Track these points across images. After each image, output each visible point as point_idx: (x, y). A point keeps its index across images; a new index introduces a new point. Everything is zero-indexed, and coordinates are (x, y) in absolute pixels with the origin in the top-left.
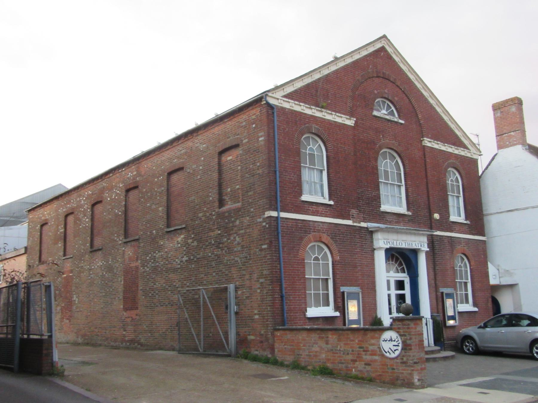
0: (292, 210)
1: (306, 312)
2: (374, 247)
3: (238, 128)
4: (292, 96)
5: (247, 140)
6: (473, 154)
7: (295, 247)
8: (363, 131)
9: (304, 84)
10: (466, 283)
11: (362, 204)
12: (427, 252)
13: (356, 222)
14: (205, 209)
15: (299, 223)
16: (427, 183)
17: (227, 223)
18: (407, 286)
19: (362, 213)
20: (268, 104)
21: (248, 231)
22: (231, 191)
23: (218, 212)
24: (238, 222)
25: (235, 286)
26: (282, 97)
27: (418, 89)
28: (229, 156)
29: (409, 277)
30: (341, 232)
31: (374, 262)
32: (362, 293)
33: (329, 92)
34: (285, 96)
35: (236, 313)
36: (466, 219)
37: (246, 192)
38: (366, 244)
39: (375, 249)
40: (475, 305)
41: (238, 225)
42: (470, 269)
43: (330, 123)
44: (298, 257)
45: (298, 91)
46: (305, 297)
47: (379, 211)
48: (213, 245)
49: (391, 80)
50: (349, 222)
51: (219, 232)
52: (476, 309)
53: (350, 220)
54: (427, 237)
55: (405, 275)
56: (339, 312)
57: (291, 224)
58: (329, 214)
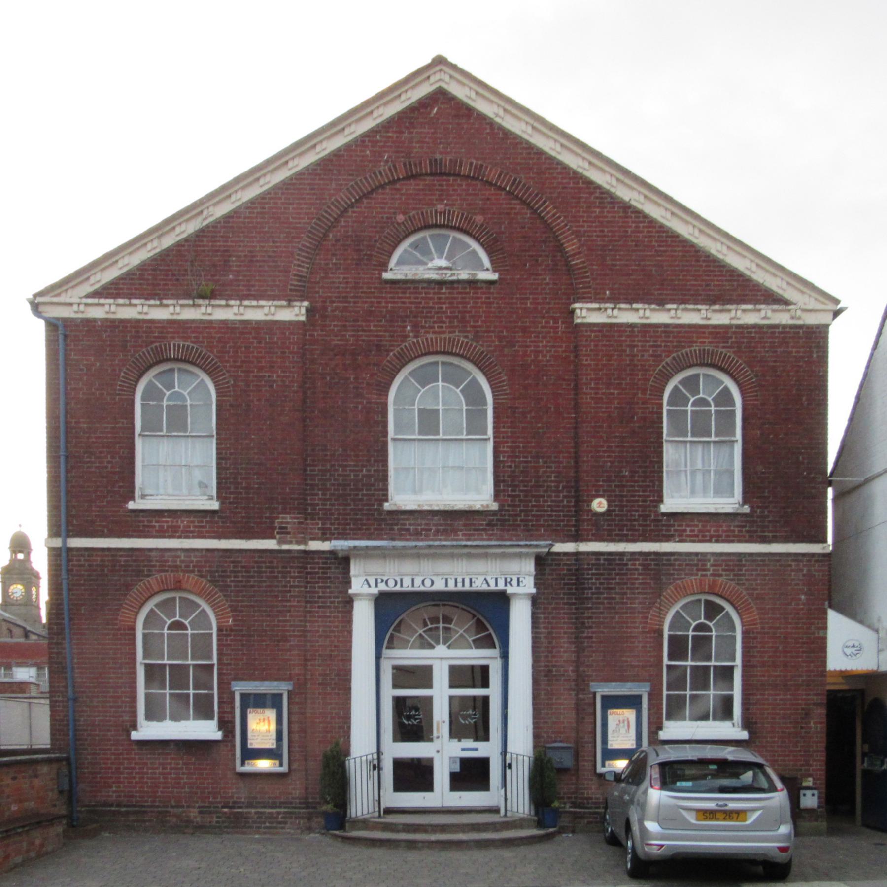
0: (103, 531)
4: (116, 289)
6: (799, 313)
11: (320, 499)
13: (291, 542)
15: (121, 556)
19: (319, 519)
33: (230, 256)
36: (746, 500)
43: (228, 328)
44: (116, 624)
45: (135, 274)
47: (380, 511)
50: (270, 544)
53: (273, 537)
57: (99, 559)
58: (207, 532)
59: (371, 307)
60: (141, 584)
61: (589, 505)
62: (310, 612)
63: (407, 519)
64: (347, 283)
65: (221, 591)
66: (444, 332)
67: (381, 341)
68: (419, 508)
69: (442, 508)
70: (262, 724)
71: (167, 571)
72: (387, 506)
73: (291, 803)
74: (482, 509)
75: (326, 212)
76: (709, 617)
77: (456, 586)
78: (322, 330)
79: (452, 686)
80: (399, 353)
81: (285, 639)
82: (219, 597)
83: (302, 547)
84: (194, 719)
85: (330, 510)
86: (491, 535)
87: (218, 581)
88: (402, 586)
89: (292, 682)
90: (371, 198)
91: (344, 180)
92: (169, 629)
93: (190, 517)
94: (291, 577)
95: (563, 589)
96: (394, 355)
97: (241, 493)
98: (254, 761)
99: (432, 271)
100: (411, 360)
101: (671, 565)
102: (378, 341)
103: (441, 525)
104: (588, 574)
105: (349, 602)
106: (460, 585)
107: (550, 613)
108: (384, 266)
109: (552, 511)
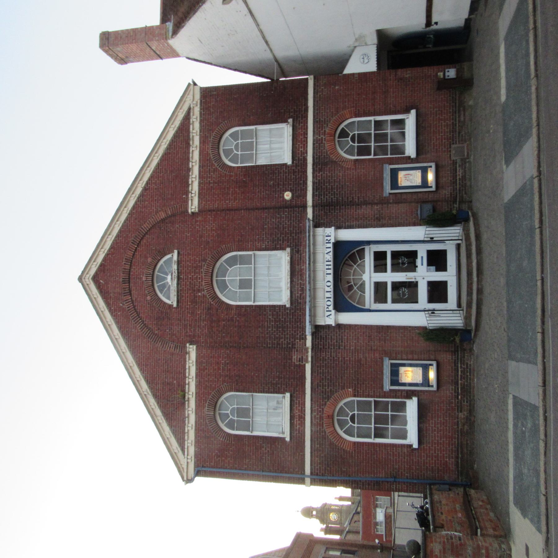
0: (302, 455)
7: (341, 455)
9: (164, 421)
11: (285, 340)
13: (307, 356)
16: (246, 209)
19: (295, 341)
38: (331, 337)
44: (352, 452)
47: (290, 309)
50: (308, 367)
53: (305, 365)
58: (302, 400)
59: (189, 313)
60: (330, 437)
62: (345, 347)
63: (295, 295)
64: (178, 324)
65: (333, 394)
66: (202, 276)
67: (206, 308)
68: (289, 289)
69: (289, 277)
70: (408, 375)
71: (323, 423)
72: (288, 305)
73: (455, 360)
74: (290, 256)
75: (145, 334)
76: (347, 135)
77: (330, 269)
78: (201, 337)
79: (386, 271)
80: (211, 299)
81: (359, 361)
82: (336, 395)
83: (310, 350)
85: (290, 335)
86: (303, 251)
87: (328, 396)
88: (330, 298)
89: (384, 358)
90: (140, 312)
91: (131, 325)
92: (354, 423)
93: (294, 409)
94: (326, 356)
95: (332, 213)
96: (213, 301)
97: (281, 381)
98: (430, 380)
99: (173, 283)
100: (215, 293)
101: (319, 157)
102: (206, 310)
103: (298, 277)
104: (324, 200)
105: (339, 326)
106: (330, 267)
107: (345, 220)
108: (170, 306)
109: (291, 220)
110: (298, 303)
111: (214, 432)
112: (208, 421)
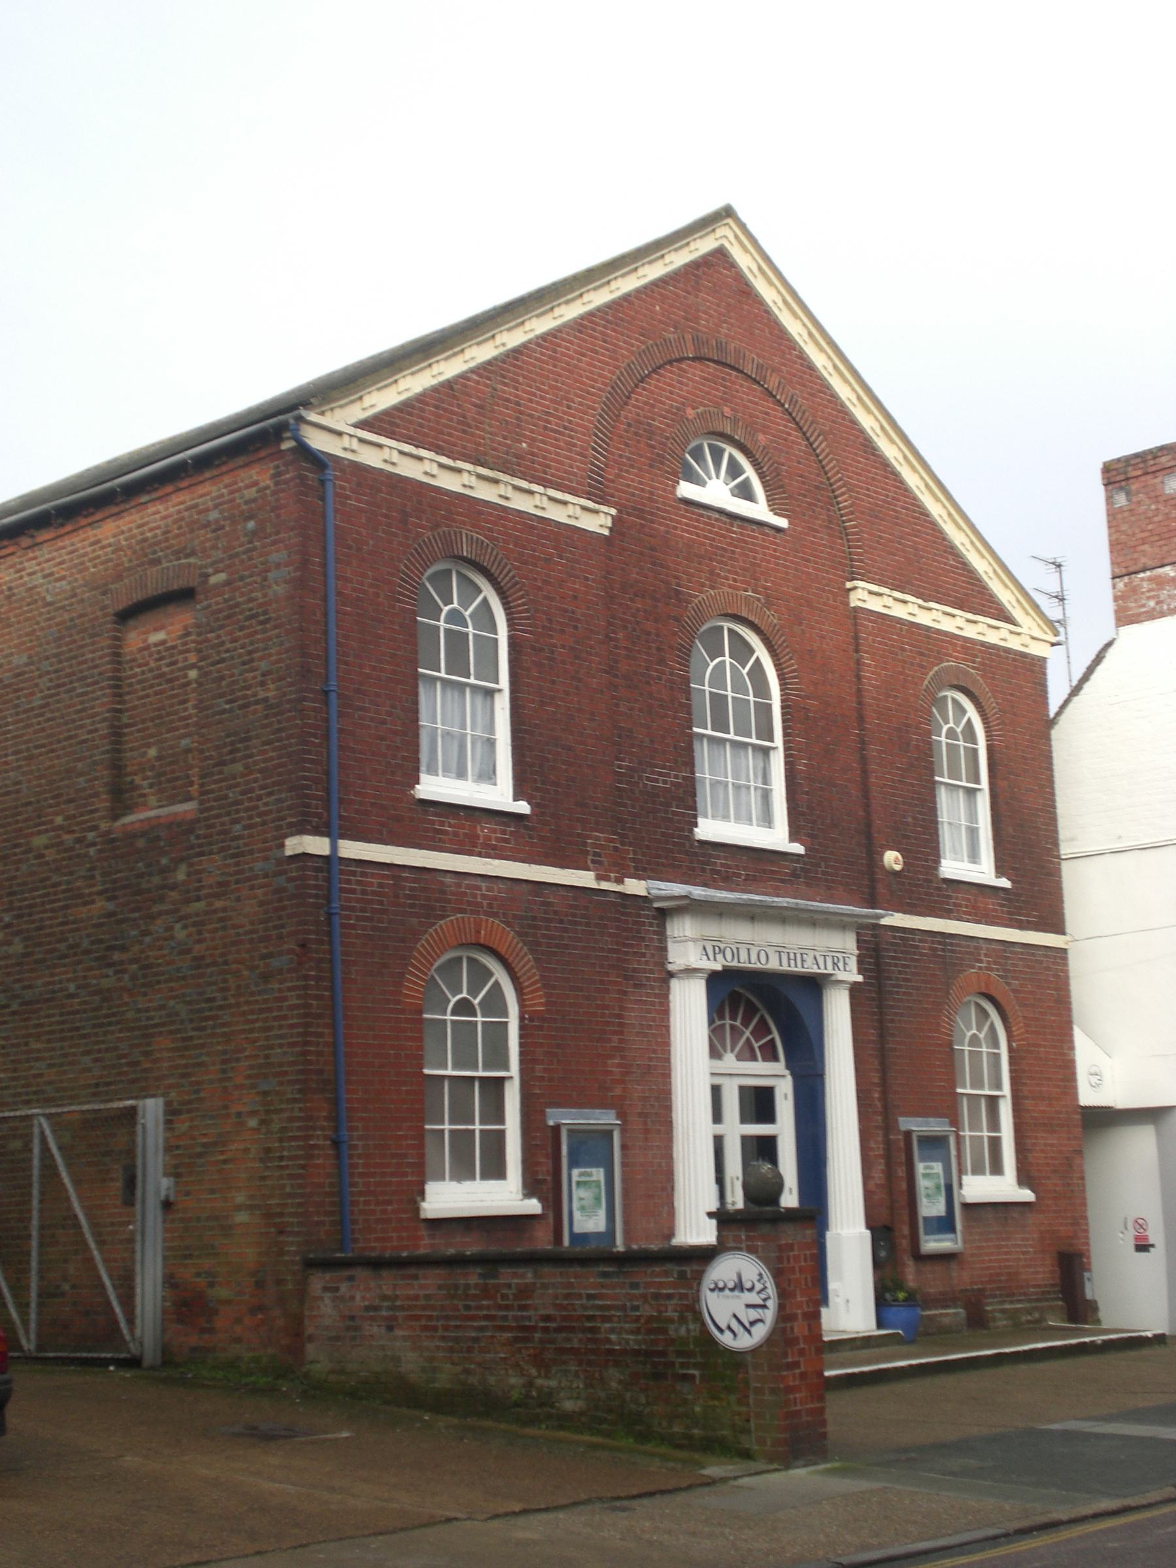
1: (423, 1199)
2: (670, 967)
3: (192, 531)
5: (222, 577)
6: (1029, 641)
8: (642, 553)
10: (993, 1101)
12: (855, 991)
13: (608, 879)
14: (59, 820)
17: (140, 876)
18: (785, 1108)
19: (630, 844)
20: (304, 452)
21: (219, 904)
22: (158, 758)
23: (109, 832)
24: (181, 876)
25: (168, 1104)
26: (356, 426)
27: (843, 405)
28: (156, 630)
29: (792, 1074)
30: (556, 912)
31: (668, 1020)
32: (624, 1131)
34: (363, 425)
35: (167, 1205)
37: (216, 765)
39: (671, 975)
40: (1025, 1177)
41: (184, 882)
42: (1011, 1050)
45: (413, 407)
46: (421, 1146)
48: (87, 952)
49: (747, 370)
51: (110, 906)
52: (1027, 1195)
53: (588, 869)
54: (858, 934)
55: (779, 1067)
56: (541, 1200)
61: (882, 860)
63: (718, 857)
84: (451, 1179)
110: (704, 863)
111: (419, 545)
112: (444, 532)
